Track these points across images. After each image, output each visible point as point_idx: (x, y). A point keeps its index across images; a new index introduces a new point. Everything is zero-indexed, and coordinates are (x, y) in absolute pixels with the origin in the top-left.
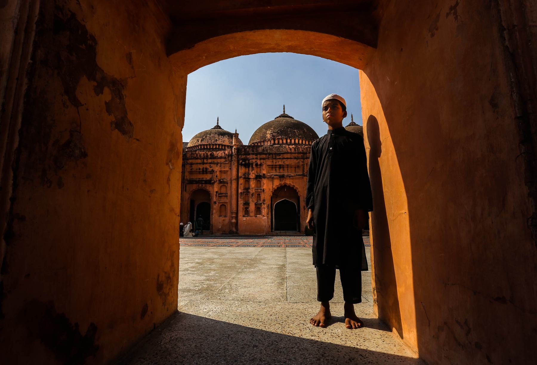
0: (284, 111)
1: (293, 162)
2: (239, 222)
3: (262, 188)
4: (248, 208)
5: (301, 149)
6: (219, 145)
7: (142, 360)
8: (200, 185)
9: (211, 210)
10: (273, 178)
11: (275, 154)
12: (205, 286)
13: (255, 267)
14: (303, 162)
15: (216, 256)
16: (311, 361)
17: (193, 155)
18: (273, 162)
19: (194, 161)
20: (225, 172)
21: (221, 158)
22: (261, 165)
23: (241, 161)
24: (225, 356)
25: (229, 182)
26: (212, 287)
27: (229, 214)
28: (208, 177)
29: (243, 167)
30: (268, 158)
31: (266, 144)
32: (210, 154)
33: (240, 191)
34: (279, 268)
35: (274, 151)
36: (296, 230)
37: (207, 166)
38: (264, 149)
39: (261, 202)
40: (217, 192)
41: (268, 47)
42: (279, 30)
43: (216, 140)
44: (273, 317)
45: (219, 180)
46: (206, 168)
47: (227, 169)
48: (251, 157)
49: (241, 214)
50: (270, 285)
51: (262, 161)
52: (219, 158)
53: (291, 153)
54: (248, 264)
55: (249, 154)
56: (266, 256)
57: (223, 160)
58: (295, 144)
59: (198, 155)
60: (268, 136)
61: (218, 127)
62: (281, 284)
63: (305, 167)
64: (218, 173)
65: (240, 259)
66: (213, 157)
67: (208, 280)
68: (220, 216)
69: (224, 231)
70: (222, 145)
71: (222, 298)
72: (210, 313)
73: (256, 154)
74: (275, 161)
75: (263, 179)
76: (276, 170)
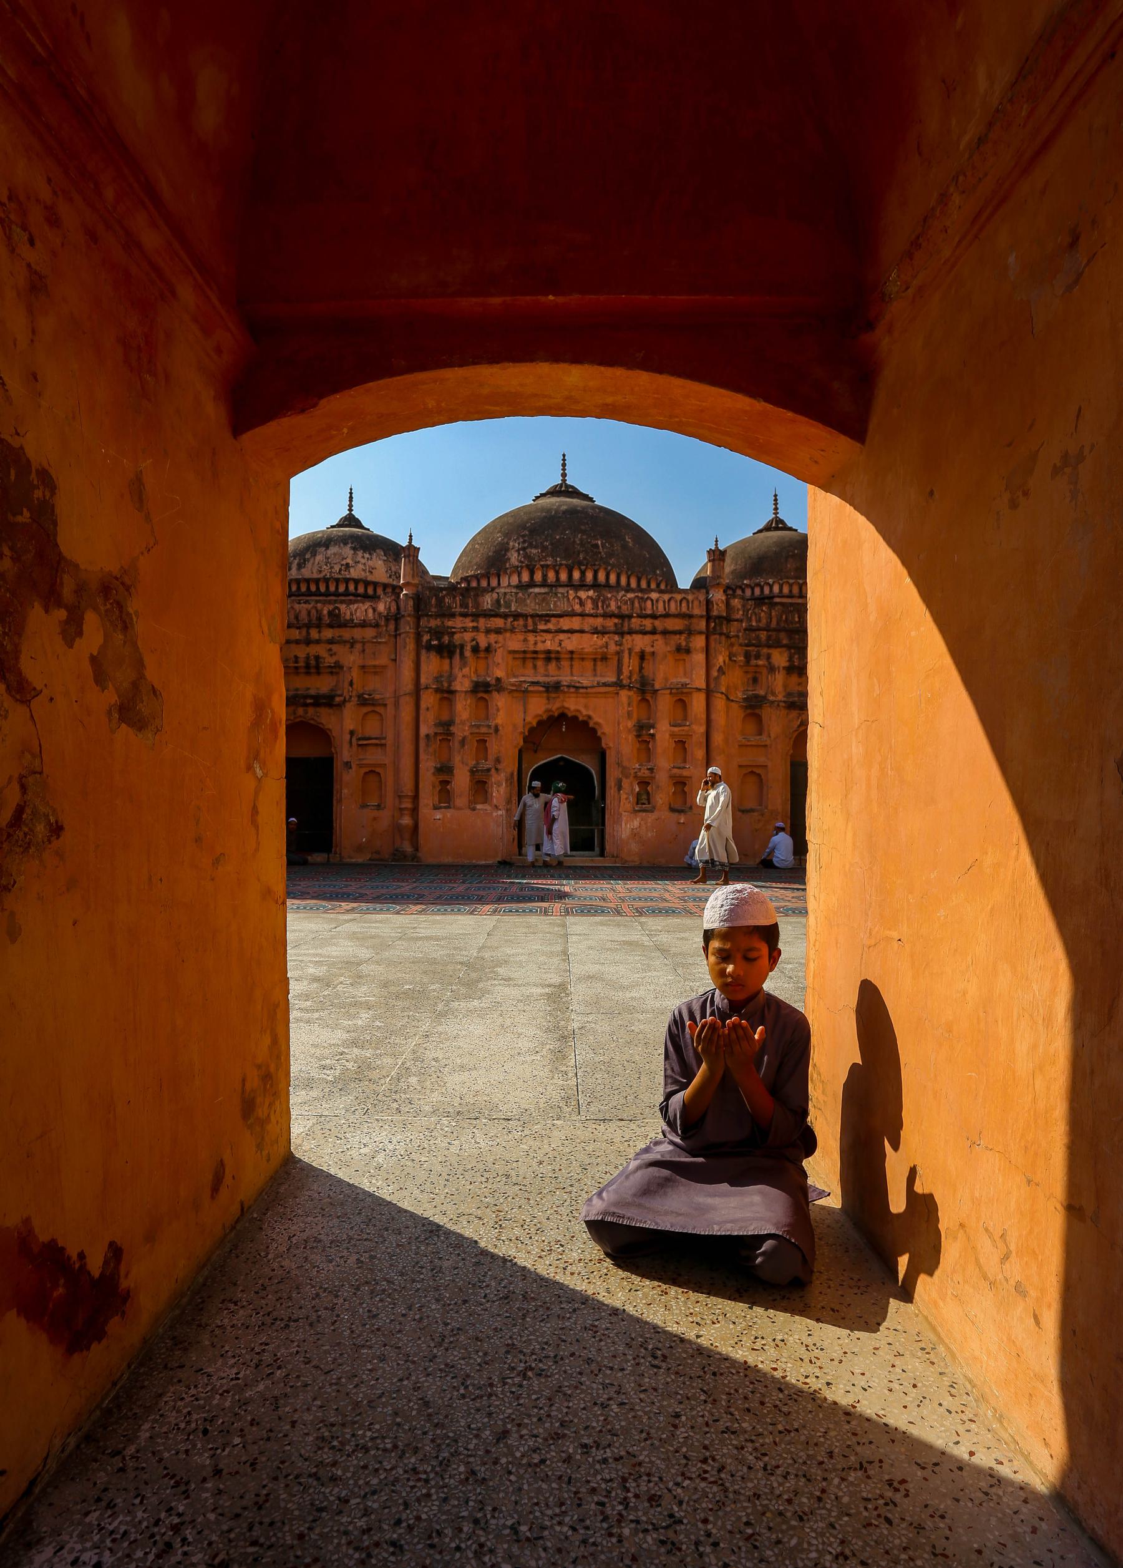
0: (564, 475)
1: (589, 643)
2: (421, 825)
3: (493, 724)
4: (448, 782)
5: (613, 606)
6: (356, 582)
7: (232, 1306)
8: (300, 711)
9: (336, 787)
10: (526, 691)
11: (532, 616)
12: (350, 1065)
13: (485, 992)
15: (364, 953)
16: (645, 1296)
20: (378, 670)
21: (364, 624)
22: (488, 650)
23: (426, 638)
24: (437, 1289)
25: (390, 702)
26: (369, 1067)
27: (390, 799)
29: (433, 656)
30: (512, 630)
31: (505, 581)
32: (330, 613)
33: (424, 730)
34: (549, 996)
35: (531, 607)
36: (592, 849)
37: (320, 650)
38: (498, 601)
40: (352, 733)
41: (541, 404)
42: (579, 366)
44: (546, 1169)
45: (360, 696)
46: (317, 658)
47: (383, 660)
48: (458, 623)
49: (428, 798)
50: (528, 1059)
51: (493, 637)
52: (356, 626)
53: (582, 615)
54: (461, 982)
55: (453, 615)
56: (509, 951)
57: (370, 633)
58: (595, 585)
60: (514, 558)
61: (350, 520)
62: (559, 1056)
63: (626, 660)
64: (355, 674)
65: (434, 962)
66: (337, 621)
67: (354, 1043)
68: (364, 806)
69: (378, 852)
70: (367, 583)
71: (404, 1109)
72: (380, 1158)
73: (476, 616)
74: (531, 638)
75: (495, 694)
76: (535, 667)
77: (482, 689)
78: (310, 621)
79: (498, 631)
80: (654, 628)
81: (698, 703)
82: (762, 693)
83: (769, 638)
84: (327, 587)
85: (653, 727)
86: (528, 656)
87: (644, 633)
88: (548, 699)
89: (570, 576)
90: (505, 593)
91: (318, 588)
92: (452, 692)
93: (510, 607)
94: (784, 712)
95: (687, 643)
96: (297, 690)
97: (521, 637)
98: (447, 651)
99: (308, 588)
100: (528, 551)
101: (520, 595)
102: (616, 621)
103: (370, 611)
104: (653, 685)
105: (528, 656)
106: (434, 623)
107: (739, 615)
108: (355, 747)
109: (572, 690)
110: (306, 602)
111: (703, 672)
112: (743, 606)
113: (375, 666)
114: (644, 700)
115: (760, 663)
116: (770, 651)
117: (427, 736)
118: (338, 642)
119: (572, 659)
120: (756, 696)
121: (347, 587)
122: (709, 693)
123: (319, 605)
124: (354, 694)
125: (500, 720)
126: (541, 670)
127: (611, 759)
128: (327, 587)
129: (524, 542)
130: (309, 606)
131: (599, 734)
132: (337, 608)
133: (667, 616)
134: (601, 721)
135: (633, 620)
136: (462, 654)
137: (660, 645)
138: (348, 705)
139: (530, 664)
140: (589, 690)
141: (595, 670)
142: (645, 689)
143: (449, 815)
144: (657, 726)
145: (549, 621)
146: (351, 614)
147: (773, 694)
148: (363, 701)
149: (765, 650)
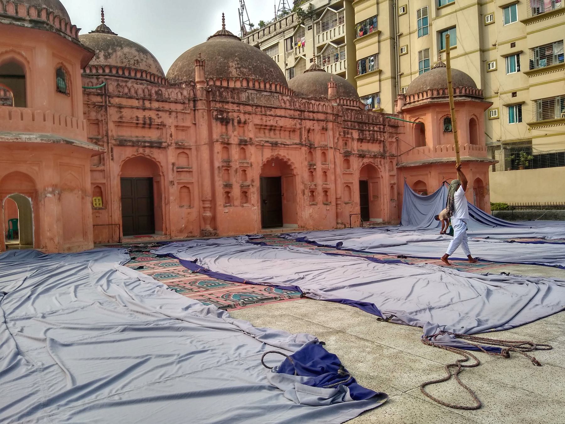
1: (288, 123)
2: (219, 217)
3: (249, 162)
5: (297, 104)
8: (141, 150)
11: (264, 107)
17: (121, 90)
18: (262, 119)
19: (124, 102)
20: (184, 129)
22: (245, 123)
23: (215, 113)
25: (193, 148)
28: (153, 135)
32: (157, 93)
33: (217, 164)
35: (263, 102)
37: (152, 114)
38: (248, 97)
39: (248, 182)
40: (173, 164)
45: (176, 143)
46: (150, 119)
47: (188, 123)
48: (230, 107)
51: (247, 116)
55: (228, 102)
57: (180, 107)
59: (133, 91)
63: (303, 132)
64: (173, 130)
66: (161, 99)
68: (181, 207)
73: (239, 104)
74: (264, 118)
75: (249, 146)
76: (265, 133)
77: (243, 144)
78: (144, 96)
80: (314, 118)
81: (330, 154)
82: (349, 150)
83: (351, 124)
84: (130, 73)
86: (263, 127)
87: (310, 120)
88: (272, 150)
89: (265, 86)
91: (124, 73)
92: (228, 144)
95: (327, 126)
96: (137, 137)
97: (260, 117)
98: (225, 122)
99: (117, 72)
100: (242, 69)
101: (258, 95)
102: (299, 113)
103: (179, 94)
104: (314, 145)
105: (263, 127)
106: (218, 105)
107: (340, 114)
109: (283, 146)
110: (141, 84)
111: (332, 140)
112: (342, 110)
113: (183, 126)
114: (310, 152)
115: (349, 136)
117: (219, 167)
118: (163, 111)
121: (142, 76)
122: (335, 149)
123: (149, 87)
124: (173, 142)
125: (253, 159)
126: (267, 134)
127: (298, 180)
128: (130, 73)
130: (144, 87)
131: (293, 167)
132: (160, 90)
133: (318, 112)
134: (294, 162)
135: (306, 113)
136: (233, 124)
137: (317, 127)
138: (170, 148)
140: (290, 146)
141: (290, 136)
142: (311, 148)
143: (231, 210)
144: (317, 164)
145: (271, 110)
146: (169, 95)
147: (354, 150)
149: (350, 131)
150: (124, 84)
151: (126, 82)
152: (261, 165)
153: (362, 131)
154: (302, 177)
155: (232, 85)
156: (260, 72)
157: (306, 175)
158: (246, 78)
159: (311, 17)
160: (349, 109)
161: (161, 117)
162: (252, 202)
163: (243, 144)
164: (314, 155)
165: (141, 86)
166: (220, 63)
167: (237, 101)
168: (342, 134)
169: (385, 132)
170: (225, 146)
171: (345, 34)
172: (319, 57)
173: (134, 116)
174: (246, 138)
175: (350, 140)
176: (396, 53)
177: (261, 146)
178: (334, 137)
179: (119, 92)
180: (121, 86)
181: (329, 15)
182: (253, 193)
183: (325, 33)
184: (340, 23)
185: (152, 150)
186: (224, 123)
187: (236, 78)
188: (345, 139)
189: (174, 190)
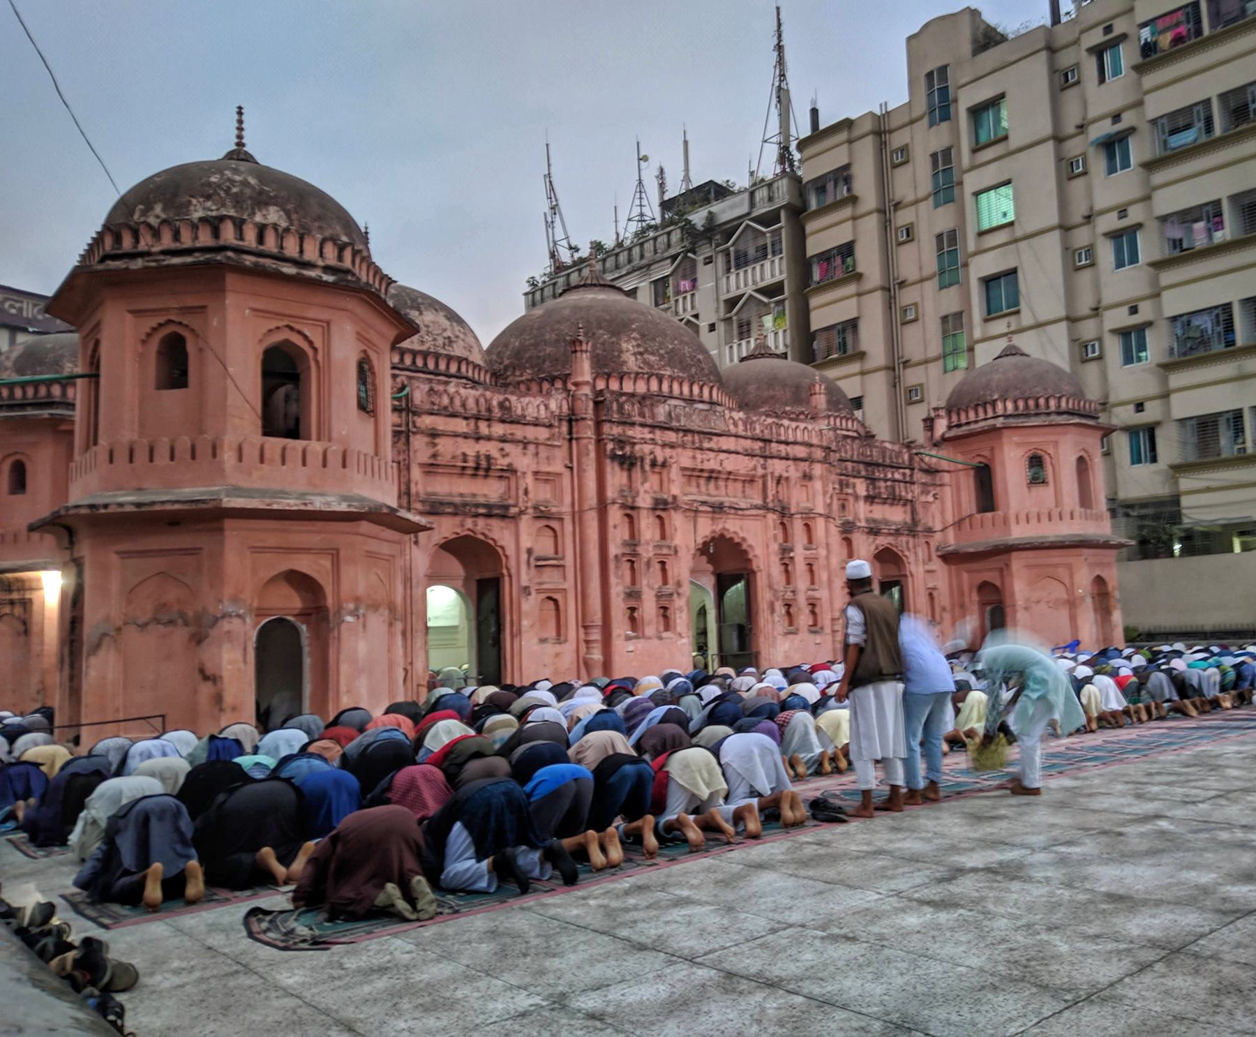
5: (758, 427)
8: (469, 523)
10: (696, 511)
11: (699, 432)
14: (764, 468)
17: (435, 399)
19: (441, 423)
22: (664, 465)
23: (610, 446)
28: (491, 490)
29: (617, 468)
30: (683, 446)
32: (501, 405)
33: (613, 550)
37: (491, 448)
38: (670, 414)
39: (670, 588)
40: (530, 551)
43: (450, 341)
45: (536, 508)
46: (488, 458)
47: (558, 466)
48: (637, 433)
49: (620, 627)
51: (668, 451)
53: (736, 436)
55: (633, 424)
57: (542, 433)
59: (457, 402)
60: (632, 363)
63: (769, 483)
64: (529, 479)
66: (509, 418)
68: (543, 641)
73: (653, 427)
74: (699, 455)
75: (672, 512)
76: (698, 486)
79: (672, 446)
81: (820, 526)
82: (851, 518)
84: (437, 364)
85: (792, 550)
87: (781, 458)
88: (713, 519)
89: (691, 391)
90: (675, 406)
92: (633, 508)
93: (679, 421)
94: (864, 537)
96: (461, 495)
97: (690, 453)
98: (628, 463)
100: (646, 356)
102: (761, 444)
103: (542, 408)
106: (617, 430)
107: (834, 448)
108: (533, 571)
113: (548, 473)
115: (850, 491)
116: (856, 480)
117: (616, 556)
118: (512, 441)
119: (727, 479)
120: (848, 522)
121: (459, 368)
122: (827, 517)
123: (488, 394)
124: (529, 504)
126: (703, 489)
127: (761, 580)
128: (437, 364)
129: (638, 346)
131: (751, 556)
132: (507, 399)
133: (795, 443)
135: (773, 445)
136: (642, 467)
137: (793, 472)
138: (525, 518)
139: (694, 483)
142: (784, 513)
146: (523, 409)
147: (859, 520)
148: (542, 514)
149: (852, 480)
150: (441, 388)
151: (447, 383)
152: (693, 551)
153: (872, 480)
154: (769, 576)
155: (628, 387)
156: (681, 362)
157: (777, 571)
158: (657, 375)
159: (710, 240)
160: (847, 437)
161: (507, 455)
162: (679, 629)
163: (662, 506)
164: (790, 531)
165: (473, 392)
166: (603, 344)
167: (649, 421)
168: (837, 486)
169: (913, 483)
170: (628, 512)
171: (784, 276)
172: (728, 320)
173: (459, 452)
174: (665, 496)
175: (851, 499)
176: (899, 318)
177: (693, 512)
178: (825, 493)
179: (433, 404)
180: (436, 393)
181: (750, 235)
182: (680, 609)
183: (741, 272)
184: (774, 253)
185: (490, 521)
186: (626, 466)
187: (637, 374)
188: (843, 496)
189: (530, 605)
